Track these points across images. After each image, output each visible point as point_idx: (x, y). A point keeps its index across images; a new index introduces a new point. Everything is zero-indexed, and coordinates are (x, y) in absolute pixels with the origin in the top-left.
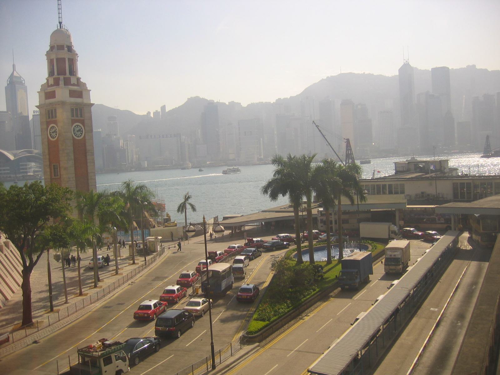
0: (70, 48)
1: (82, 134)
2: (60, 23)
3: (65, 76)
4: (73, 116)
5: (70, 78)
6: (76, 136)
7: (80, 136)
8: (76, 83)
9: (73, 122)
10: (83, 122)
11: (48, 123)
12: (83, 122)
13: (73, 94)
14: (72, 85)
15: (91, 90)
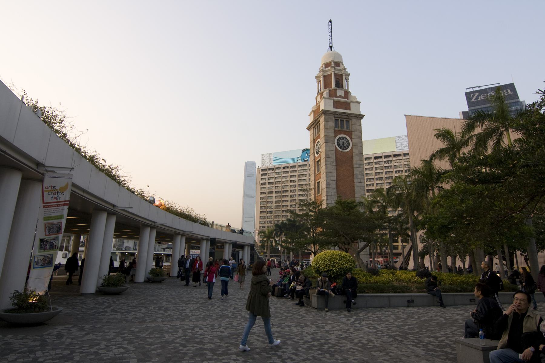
0: (338, 64)
1: (348, 147)
2: (331, 47)
3: (331, 89)
4: (336, 125)
5: (335, 90)
6: (340, 148)
7: (346, 149)
8: (343, 95)
9: (336, 133)
10: (350, 134)
11: (314, 141)
12: (350, 134)
13: (337, 104)
14: (336, 96)
15: (360, 103)
